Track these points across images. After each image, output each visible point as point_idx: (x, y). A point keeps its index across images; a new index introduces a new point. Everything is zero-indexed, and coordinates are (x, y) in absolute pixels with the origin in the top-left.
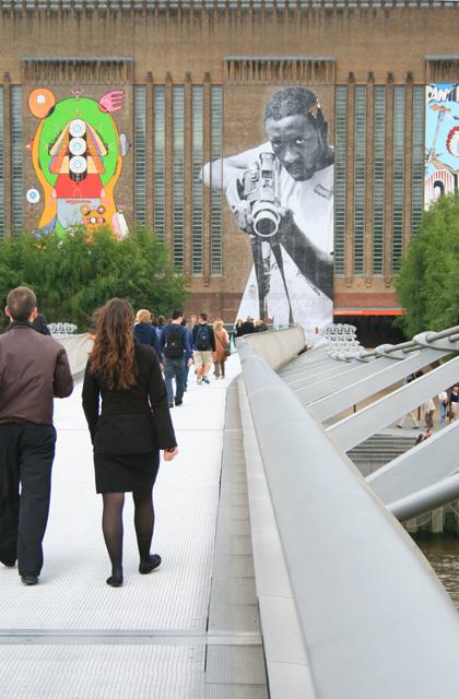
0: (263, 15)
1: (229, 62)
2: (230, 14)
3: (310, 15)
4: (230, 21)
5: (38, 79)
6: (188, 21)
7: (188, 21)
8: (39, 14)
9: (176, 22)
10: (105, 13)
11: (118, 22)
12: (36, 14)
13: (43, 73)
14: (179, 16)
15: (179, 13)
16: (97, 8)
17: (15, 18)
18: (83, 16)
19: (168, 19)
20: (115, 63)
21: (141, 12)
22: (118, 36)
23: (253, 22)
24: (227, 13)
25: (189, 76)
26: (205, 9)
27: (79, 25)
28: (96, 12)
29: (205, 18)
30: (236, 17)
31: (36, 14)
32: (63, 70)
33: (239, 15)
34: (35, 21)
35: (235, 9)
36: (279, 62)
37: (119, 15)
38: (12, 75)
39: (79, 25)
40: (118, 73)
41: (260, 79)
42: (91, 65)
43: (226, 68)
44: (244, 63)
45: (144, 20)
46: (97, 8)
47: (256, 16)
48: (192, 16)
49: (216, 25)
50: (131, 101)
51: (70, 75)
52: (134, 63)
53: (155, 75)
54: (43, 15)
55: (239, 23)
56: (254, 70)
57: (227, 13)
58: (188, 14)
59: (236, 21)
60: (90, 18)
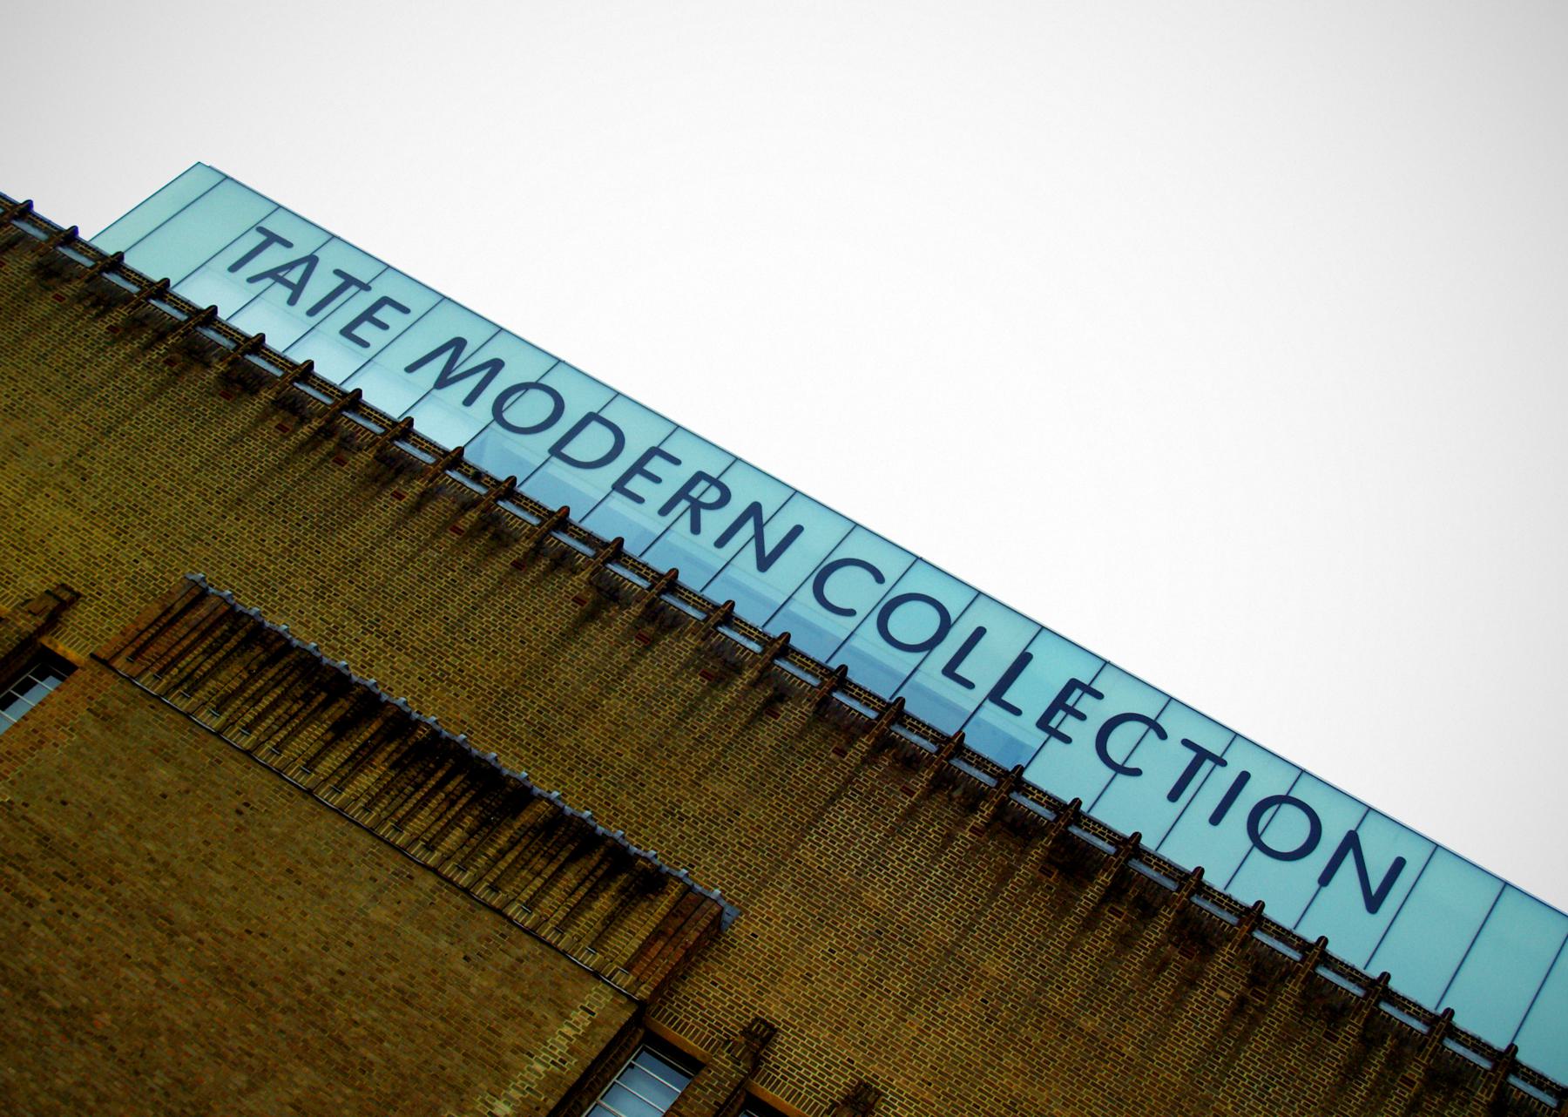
4: (1352, 1071)
6: (1125, 941)
7: (1125, 941)
8: (426, 497)
9: (1062, 907)
10: (737, 669)
11: (767, 735)
12: (419, 486)
13: (230, 678)
14: (1092, 892)
15: (1104, 878)
17: (302, 447)
18: (624, 618)
19: (1025, 871)
20: (619, 858)
22: (722, 788)
24: (1352, 1028)
26: (1248, 939)
28: (692, 641)
30: (1395, 1062)
31: (419, 486)
32: (340, 730)
33: (1416, 1072)
34: (386, 509)
35: (1405, 1036)
37: (793, 715)
38: (81, 617)
48: (1155, 933)
49: (1262, 1040)
50: (573, 1069)
51: (358, 762)
53: (789, 1052)
54: (437, 509)
57: (1352, 1028)
59: (1380, 1091)
60: (649, 643)
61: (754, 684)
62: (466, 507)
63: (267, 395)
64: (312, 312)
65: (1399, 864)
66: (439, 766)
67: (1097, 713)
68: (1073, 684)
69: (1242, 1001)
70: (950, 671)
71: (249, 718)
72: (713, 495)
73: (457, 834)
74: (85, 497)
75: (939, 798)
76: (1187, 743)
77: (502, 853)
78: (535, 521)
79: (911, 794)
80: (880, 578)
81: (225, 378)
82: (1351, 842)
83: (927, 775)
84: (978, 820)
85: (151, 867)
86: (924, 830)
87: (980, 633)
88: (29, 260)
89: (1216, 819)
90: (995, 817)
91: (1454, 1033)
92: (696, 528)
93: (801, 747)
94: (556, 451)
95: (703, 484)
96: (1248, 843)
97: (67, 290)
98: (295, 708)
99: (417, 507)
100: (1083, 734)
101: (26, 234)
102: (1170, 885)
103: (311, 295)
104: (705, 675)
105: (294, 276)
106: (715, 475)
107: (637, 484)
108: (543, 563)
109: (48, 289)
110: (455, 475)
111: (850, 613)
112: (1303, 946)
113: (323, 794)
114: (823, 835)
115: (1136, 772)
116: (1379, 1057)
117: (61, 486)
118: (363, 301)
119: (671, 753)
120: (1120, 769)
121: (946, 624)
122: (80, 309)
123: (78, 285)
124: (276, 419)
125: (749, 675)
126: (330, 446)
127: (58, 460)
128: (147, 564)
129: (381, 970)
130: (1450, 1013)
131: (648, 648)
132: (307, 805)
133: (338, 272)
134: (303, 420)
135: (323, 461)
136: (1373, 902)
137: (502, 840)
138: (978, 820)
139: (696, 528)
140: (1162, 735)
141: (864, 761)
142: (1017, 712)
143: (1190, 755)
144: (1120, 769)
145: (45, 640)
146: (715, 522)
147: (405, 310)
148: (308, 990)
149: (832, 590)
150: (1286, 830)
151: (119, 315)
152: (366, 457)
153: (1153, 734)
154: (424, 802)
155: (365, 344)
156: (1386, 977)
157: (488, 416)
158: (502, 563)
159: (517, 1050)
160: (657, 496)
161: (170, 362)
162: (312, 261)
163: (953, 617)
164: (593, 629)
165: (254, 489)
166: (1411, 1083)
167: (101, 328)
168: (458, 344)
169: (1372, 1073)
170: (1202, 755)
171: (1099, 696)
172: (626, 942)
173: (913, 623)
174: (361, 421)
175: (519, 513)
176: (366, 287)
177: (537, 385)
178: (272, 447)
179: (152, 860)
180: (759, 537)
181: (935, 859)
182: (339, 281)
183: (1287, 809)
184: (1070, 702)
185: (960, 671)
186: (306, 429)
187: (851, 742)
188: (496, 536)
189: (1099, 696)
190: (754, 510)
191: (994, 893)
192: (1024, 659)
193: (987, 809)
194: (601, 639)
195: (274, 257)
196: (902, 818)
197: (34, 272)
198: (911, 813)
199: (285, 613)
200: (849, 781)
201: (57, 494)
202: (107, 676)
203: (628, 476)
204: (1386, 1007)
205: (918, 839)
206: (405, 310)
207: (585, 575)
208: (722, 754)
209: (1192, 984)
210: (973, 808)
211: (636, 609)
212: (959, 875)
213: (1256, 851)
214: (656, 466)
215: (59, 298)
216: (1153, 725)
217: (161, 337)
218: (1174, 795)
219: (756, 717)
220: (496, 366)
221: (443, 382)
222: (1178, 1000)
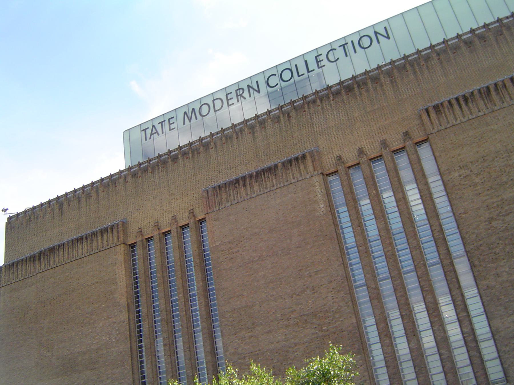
0: (450, 52)
1: (427, 110)
2: (412, 66)
3: (505, 32)
4: (415, 72)
5: (220, 203)
6: (368, 91)
7: (368, 91)
9: (355, 96)
10: (279, 117)
11: (293, 121)
12: (212, 144)
13: (224, 196)
14: (356, 89)
15: (355, 86)
16: (270, 117)
17: (193, 157)
18: (257, 128)
20: (297, 159)
21: (314, 102)
23: (441, 63)
24: (408, 67)
25: (384, 144)
26: (382, 72)
27: (254, 138)
29: (385, 80)
30: (418, 64)
31: (212, 144)
32: (244, 185)
33: (423, 63)
34: (212, 151)
35: (415, 59)
36: (488, 88)
37: (293, 114)
38: (196, 211)
39: (254, 138)
40: (302, 167)
41: (471, 114)
42: (272, 170)
43: (425, 117)
44: (446, 104)
45: (320, 107)
46: (270, 117)
47: (442, 57)
50: (324, 191)
51: (251, 187)
52: (318, 152)
55: (425, 71)
56: (460, 107)
57: (408, 67)
58: (365, 83)
60: (265, 127)
61: (283, 116)
62: (221, 139)
63: (180, 156)
64: (163, 133)
65: (385, 28)
66: (261, 175)
67: (323, 57)
68: (316, 57)
69: (391, 81)
70: (299, 76)
71: (232, 198)
72: (241, 91)
73: (274, 180)
74: (177, 197)
75: (323, 101)
76: (340, 46)
77: (282, 176)
78: (231, 130)
79: (319, 105)
80: (275, 75)
81: (172, 161)
82: (376, 33)
83: (318, 101)
84: (331, 98)
85: (245, 230)
86: (327, 108)
87: (296, 66)
88: (130, 176)
89: (355, 52)
90: (333, 95)
91: (421, 51)
92: (245, 98)
93: (299, 117)
94: (215, 111)
95: (238, 91)
96: (363, 50)
97: (139, 175)
98: (236, 190)
99: (216, 146)
100: (325, 62)
101: (125, 174)
102: (364, 77)
103: (160, 131)
104: (276, 123)
105: (154, 131)
106: (238, 88)
107: (230, 102)
108: (239, 134)
109: (137, 177)
110: (215, 137)
111: (277, 84)
112: (390, 63)
113: (253, 196)
114: (315, 125)
115: (338, 59)
116: (416, 66)
117: (172, 199)
118: (167, 122)
119: (285, 138)
120: (336, 61)
121: (291, 70)
122: (144, 175)
123: (140, 172)
124: (185, 158)
125: (281, 116)
126: (196, 153)
127: (168, 196)
128: (195, 195)
129: (287, 208)
130: (418, 49)
131: (265, 128)
132: (253, 199)
133: (159, 123)
134: (188, 154)
135: (197, 155)
136: (388, 38)
137: (280, 174)
138: (331, 98)
139: (245, 98)
140: (335, 49)
141: (309, 108)
142: (314, 70)
143: (342, 47)
144: (336, 61)
145: (197, 219)
146: (246, 94)
147: (173, 117)
148: (282, 221)
149: (271, 84)
150: (366, 42)
151: (150, 170)
152: (202, 148)
153: (334, 51)
154: (266, 182)
155: (174, 128)
156: (404, 55)
157: (201, 117)
158: (235, 141)
159: (315, 197)
160: (234, 100)
161: (164, 167)
162: (153, 126)
163: (290, 68)
164: (256, 134)
165: (194, 170)
166: (424, 65)
167: (150, 174)
168: (185, 113)
169: (417, 70)
170: (343, 46)
171: (321, 55)
172: (311, 168)
173: (287, 75)
174: (195, 145)
175: (228, 131)
176: (165, 121)
177: (202, 106)
178: (189, 162)
179: (245, 229)
180: (254, 89)
181: (333, 110)
182: (160, 124)
183: (362, 39)
184: (318, 60)
185: (300, 74)
186: (190, 154)
187: (304, 108)
188: (230, 138)
189: (321, 55)
190: (249, 86)
191: (345, 105)
192: (306, 62)
193: (331, 96)
194: (258, 134)
195: (149, 132)
196: (322, 110)
197: (133, 177)
198: (322, 108)
199: (218, 180)
200: (310, 114)
201: (174, 201)
202: (210, 214)
203: (228, 103)
204: (409, 59)
205: (327, 110)
206: (173, 117)
207: (246, 129)
208: (291, 130)
209: (382, 86)
210: (329, 98)
211: (258, 125)
212: (338, 108)
213: (366, 50)
214: (229, 97)
215: (140, 177)
216: (332, 50)
217: (158, 165)
218: (347, 56)
219: (289, 120)
220: (193, 110)
221: (190, 120)
222: (383, 90)
